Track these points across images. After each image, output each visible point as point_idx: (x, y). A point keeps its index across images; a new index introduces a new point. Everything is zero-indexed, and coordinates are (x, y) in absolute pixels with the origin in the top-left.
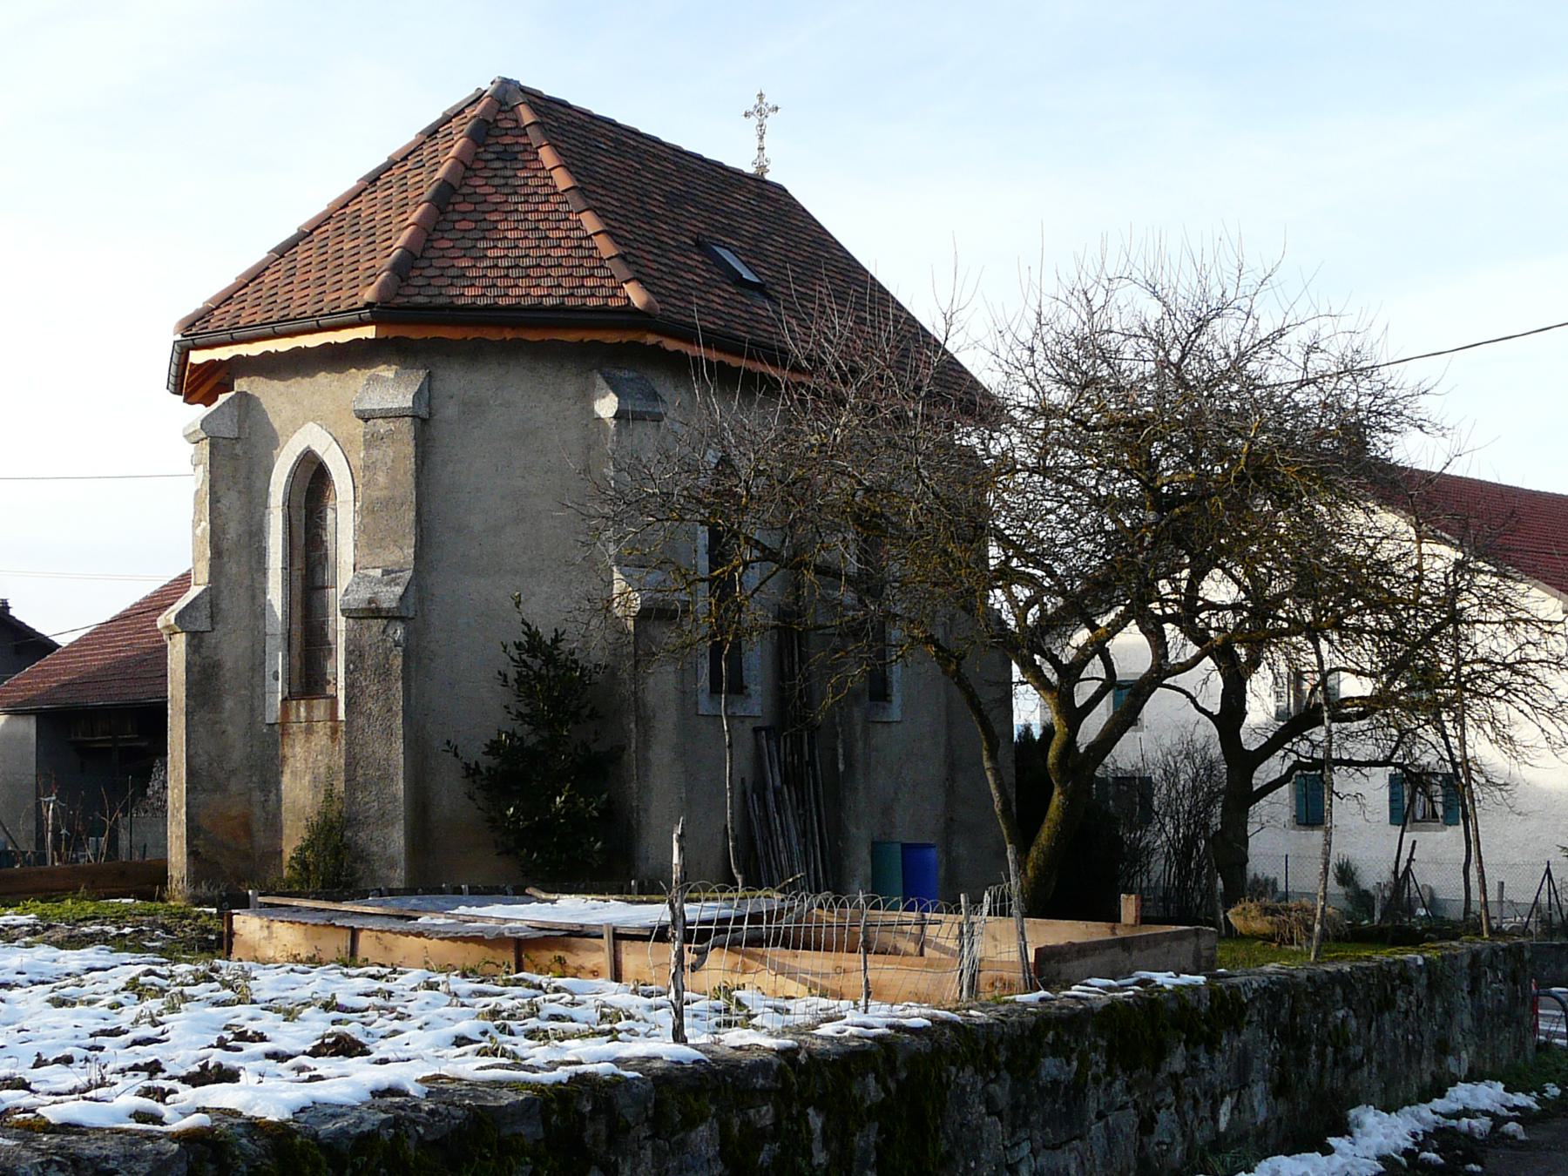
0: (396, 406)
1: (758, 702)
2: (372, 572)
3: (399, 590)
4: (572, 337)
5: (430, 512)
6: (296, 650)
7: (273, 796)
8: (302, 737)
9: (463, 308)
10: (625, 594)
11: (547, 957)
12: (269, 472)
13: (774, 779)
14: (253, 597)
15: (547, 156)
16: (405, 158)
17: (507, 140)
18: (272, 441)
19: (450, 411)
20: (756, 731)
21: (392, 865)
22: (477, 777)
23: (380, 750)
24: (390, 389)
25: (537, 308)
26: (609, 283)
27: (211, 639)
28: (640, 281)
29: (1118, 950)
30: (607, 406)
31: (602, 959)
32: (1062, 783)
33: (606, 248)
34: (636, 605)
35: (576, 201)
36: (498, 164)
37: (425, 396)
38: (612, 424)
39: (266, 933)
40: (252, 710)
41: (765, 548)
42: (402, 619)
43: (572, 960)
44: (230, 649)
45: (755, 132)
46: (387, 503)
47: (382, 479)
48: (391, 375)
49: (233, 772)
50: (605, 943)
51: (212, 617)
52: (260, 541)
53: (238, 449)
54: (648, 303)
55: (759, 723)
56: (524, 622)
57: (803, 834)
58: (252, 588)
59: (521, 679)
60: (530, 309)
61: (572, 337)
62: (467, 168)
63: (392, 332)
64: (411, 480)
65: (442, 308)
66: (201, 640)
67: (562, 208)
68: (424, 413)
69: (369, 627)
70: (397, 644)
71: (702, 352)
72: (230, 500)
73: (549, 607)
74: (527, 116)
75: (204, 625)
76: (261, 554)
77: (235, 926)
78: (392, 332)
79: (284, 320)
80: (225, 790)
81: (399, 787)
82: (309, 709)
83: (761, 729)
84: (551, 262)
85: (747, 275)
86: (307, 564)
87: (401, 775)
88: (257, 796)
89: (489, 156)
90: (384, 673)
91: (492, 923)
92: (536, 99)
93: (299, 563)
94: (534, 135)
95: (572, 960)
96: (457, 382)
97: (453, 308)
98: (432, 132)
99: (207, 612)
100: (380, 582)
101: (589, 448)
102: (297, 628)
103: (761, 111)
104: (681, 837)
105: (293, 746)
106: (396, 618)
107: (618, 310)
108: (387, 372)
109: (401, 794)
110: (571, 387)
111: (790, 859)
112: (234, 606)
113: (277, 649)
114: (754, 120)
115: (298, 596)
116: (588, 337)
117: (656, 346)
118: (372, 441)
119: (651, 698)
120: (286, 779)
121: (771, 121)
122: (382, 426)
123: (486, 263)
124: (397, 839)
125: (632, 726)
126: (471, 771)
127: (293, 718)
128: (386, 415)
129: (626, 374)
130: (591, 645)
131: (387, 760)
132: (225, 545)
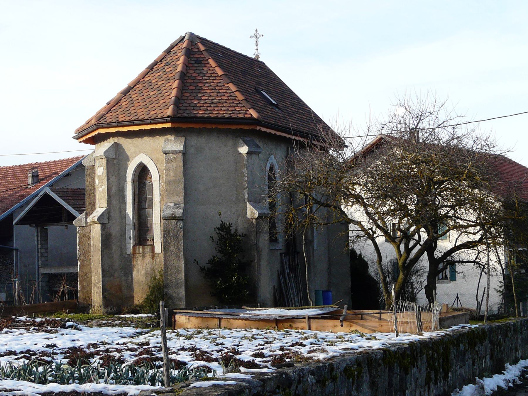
0: (177, 149)
1: (280, 246)
2: (170, 204)
3: (182, 211)
4: (234, 127)
5: (189, 184)
6: (136, 229)
7: (130, 278)
8: (141, 258)
9: (200, 118)
10: (252, 212)
11: (286, 325)
12: (126, 169)
13: (287, 270)
14: (121, 212)
15: (211, 61)
16: (161, 61)
17: (198, 56)
18: (127, 159)
19: (192, 151)
20: (281, 254)
21: (181, 300)
22: (204, 271)
23: (175, 262)
24: (174, 144)
25: (223, 118)
26: (244, 109)
27: (108, 226)
28: (254, 109)
29: (452, 319)
30: (244, 150)
31: (306, 325)
32: (403, 271)
33: (240, 97)
34: (257, 215)
35: (226, 80)
36: (196, 65)
37: (185, 146)
38: (245, 156)
39: (188, 320)
40: (121, 249)
41: (316, 200)
42: (182, 220)
43: (294, 325)
44: (115, 229)
45: (254, 43)
46: (174, 182)
47: (172, 173)
48: (173, 139)
49: (116, 270)
50: (306, 320)
51: (108, 218)
52: (123, 193)
53: (115, 162)
54: (258, 117)
55: (282, 252)
56: (221, 221)
57: (296, 288)
58: (120, 208)
59: (220, 239)
60: (221, 118)
61: (234, 127)
62: (187, 66)
63: (176, 125)
64: (182, 174)
65: (193, 118)
66: (105, 226)
67: (222, 81)
68: (184, 152)
69: (171, 223)
70: (181, 228)
71: (293, 137)
72: (113, 179)
73: (229, 216)
74: (202, 48)
75: (106, 221)
76: (123, 197)
77: (176, 319)
78: (176, 125)
79: (137, 120)
80: (113, 276)
81: (183, 275)
82: (144, 249)
83: (283, 253)
84: (223, 101)
85: (273, 102)
86: (139, 200)
87: (183, 271)
88: (124, 278)
89: (193, 62)
90: (177, 238)
91: (265, 316)
92: (204, 41)
93: (137, 201)
94: (206, 54)
95: (294, 325)
96: (196, 141)
97: (196, 118)
98: (168, 51)
99: (107, 217)
100: (173, 208)
101: (236, 163)
102: (137, 222)
103: (257, 36)
104: (394, 289)
105: (137, 262)
106: (180, 220)
107: (248, 119)
108: (171, 138)
109: (183, 277)
110: (230, 143)
111: (294, 296)
112: (115, 214)
113: (131, 229)
114: (254, 39)
115: (137, 211)
116: (239, 127)
117: (260, 130)
118: (168, 161)
119: (261, 245)
120: (135, 273)
121: (260, 40)
122: (172, 156)
123: (202, 102)
124: (182, 292)
125: (255, 254)
126: (202, 269)
127: (137, 252)
128: (173, 152)
129: (248, 139)
130: (240, 227)
131: (179, 266)
132: (112, 194)
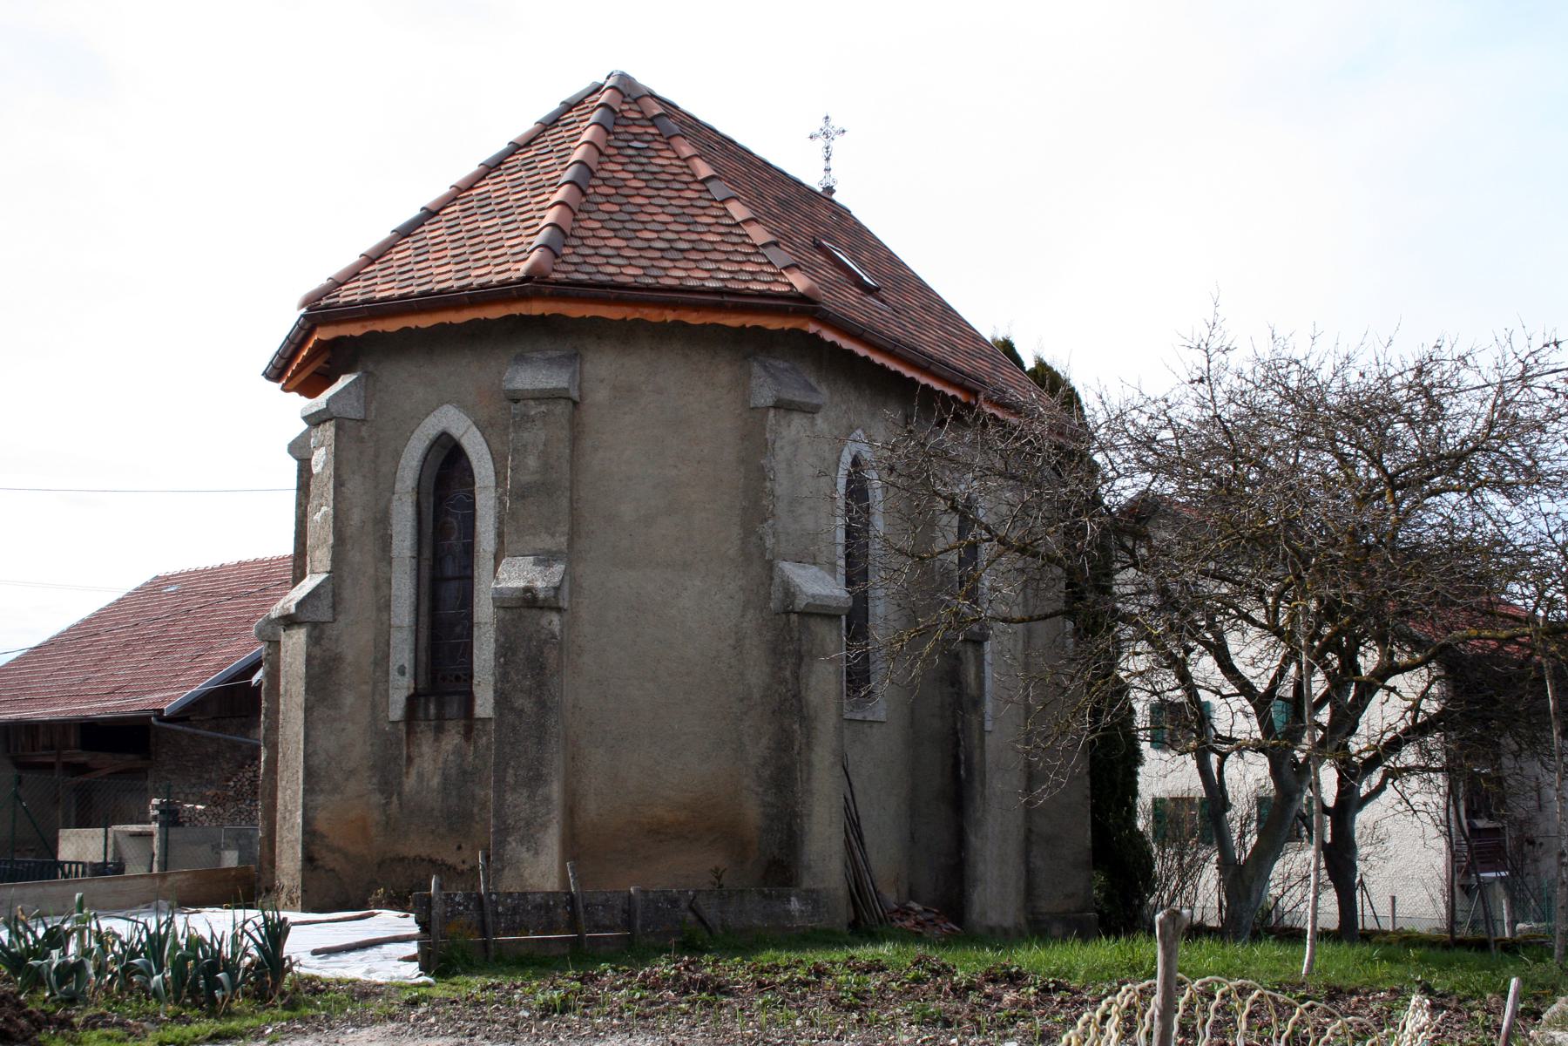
4: (733, 321)
8: (431, 735)
40: (374, 707)
45: (822, 154)
51: (334, 607)
52: (386, 529)
66: (322, 632)
72: (356, 486)
75: (324, 614)
82: (440, 707)
93: (427, 553)
98: (551, 123)
105: (419, 746)
114: (821, 142)
115: (425, 589)
116: (750, 321)
117: (816, 335)
121: (837, 144)
125: (796, 727)
